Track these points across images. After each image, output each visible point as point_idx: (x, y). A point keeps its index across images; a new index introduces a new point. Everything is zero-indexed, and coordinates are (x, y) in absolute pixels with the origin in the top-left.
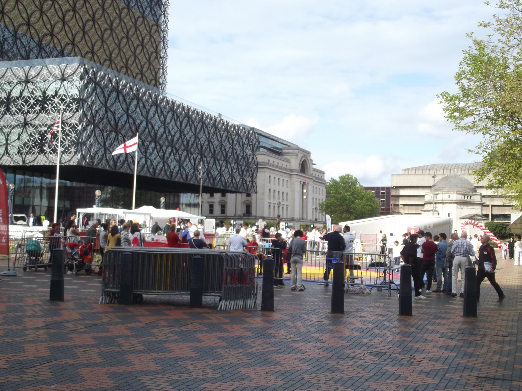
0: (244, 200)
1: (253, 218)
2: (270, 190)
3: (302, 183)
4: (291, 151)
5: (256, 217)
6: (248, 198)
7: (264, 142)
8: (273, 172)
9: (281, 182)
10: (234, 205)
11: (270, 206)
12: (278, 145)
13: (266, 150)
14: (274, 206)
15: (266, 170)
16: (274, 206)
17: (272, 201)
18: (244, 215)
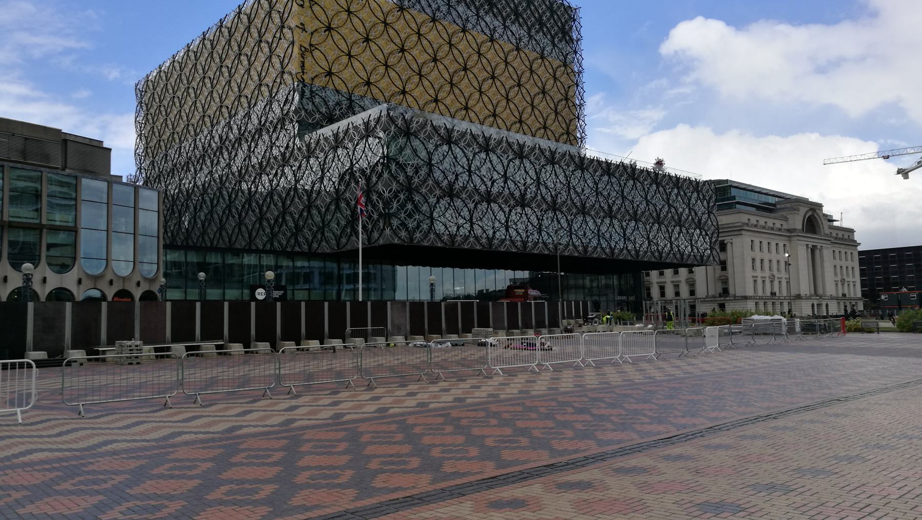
0: (717, 275)
1: (731, 298)
2: (753, 260)
3: (810, 246)
4: (788, 205)
5: (735, 296)
6: (724, 273)
7: (739, 196)
8: (757, 235)
9: (773, 247)
10: (705, 283)
11: (755, 281)
12: (771, 200)
13: (754, 209)
14: (764, 281)
15: (743, 232)
16: (764, 281)
17: (759, 273)
18: (720, 296)
